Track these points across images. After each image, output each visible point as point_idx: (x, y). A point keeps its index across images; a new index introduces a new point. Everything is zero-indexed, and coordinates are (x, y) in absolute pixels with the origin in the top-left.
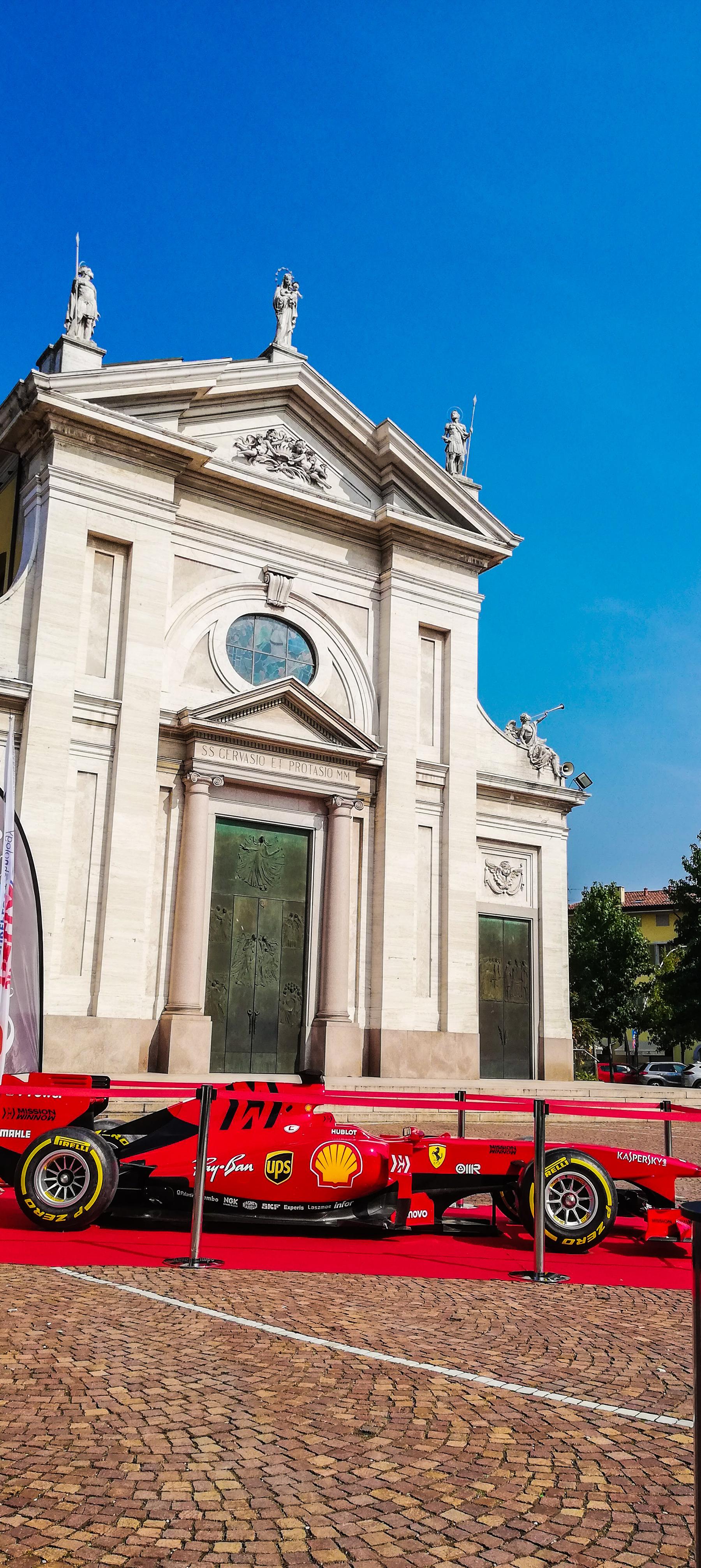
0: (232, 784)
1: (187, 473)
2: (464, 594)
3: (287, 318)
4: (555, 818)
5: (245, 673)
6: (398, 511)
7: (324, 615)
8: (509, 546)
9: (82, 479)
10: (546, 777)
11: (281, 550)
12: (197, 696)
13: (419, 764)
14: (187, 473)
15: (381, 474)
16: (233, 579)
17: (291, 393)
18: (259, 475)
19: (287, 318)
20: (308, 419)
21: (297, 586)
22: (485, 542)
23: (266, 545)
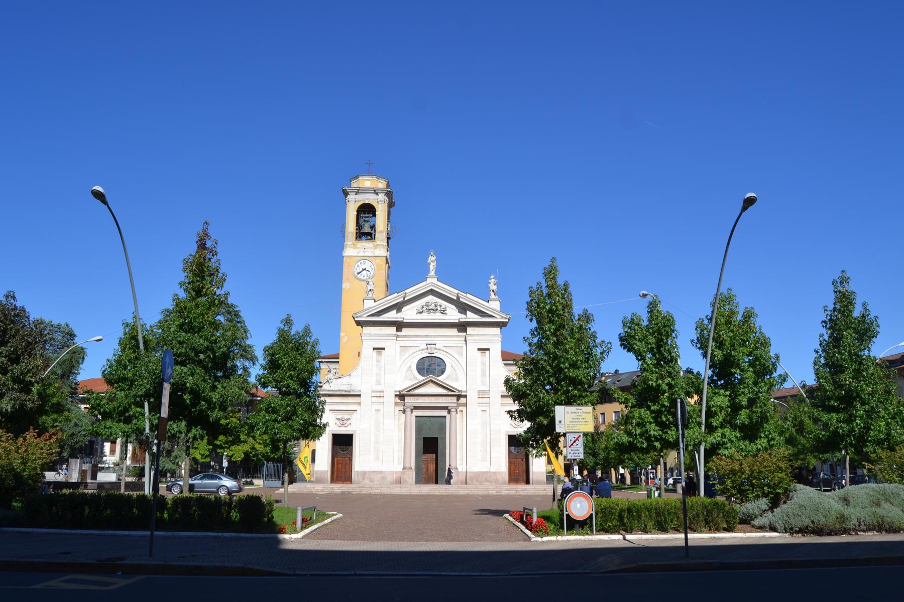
0: (416, 408)
1: (399, 326)
2: (494, 336)
3: (432, 266)
5: (423, 375)
6: (471, 317)
11: (431, 336)
12: (403, 385)
13: (479, 392)
14: (399, 326)
15: (463, 308)
19: (432, 266)
21: (437, 347)
22: (498, 319)
23: (427, 336)
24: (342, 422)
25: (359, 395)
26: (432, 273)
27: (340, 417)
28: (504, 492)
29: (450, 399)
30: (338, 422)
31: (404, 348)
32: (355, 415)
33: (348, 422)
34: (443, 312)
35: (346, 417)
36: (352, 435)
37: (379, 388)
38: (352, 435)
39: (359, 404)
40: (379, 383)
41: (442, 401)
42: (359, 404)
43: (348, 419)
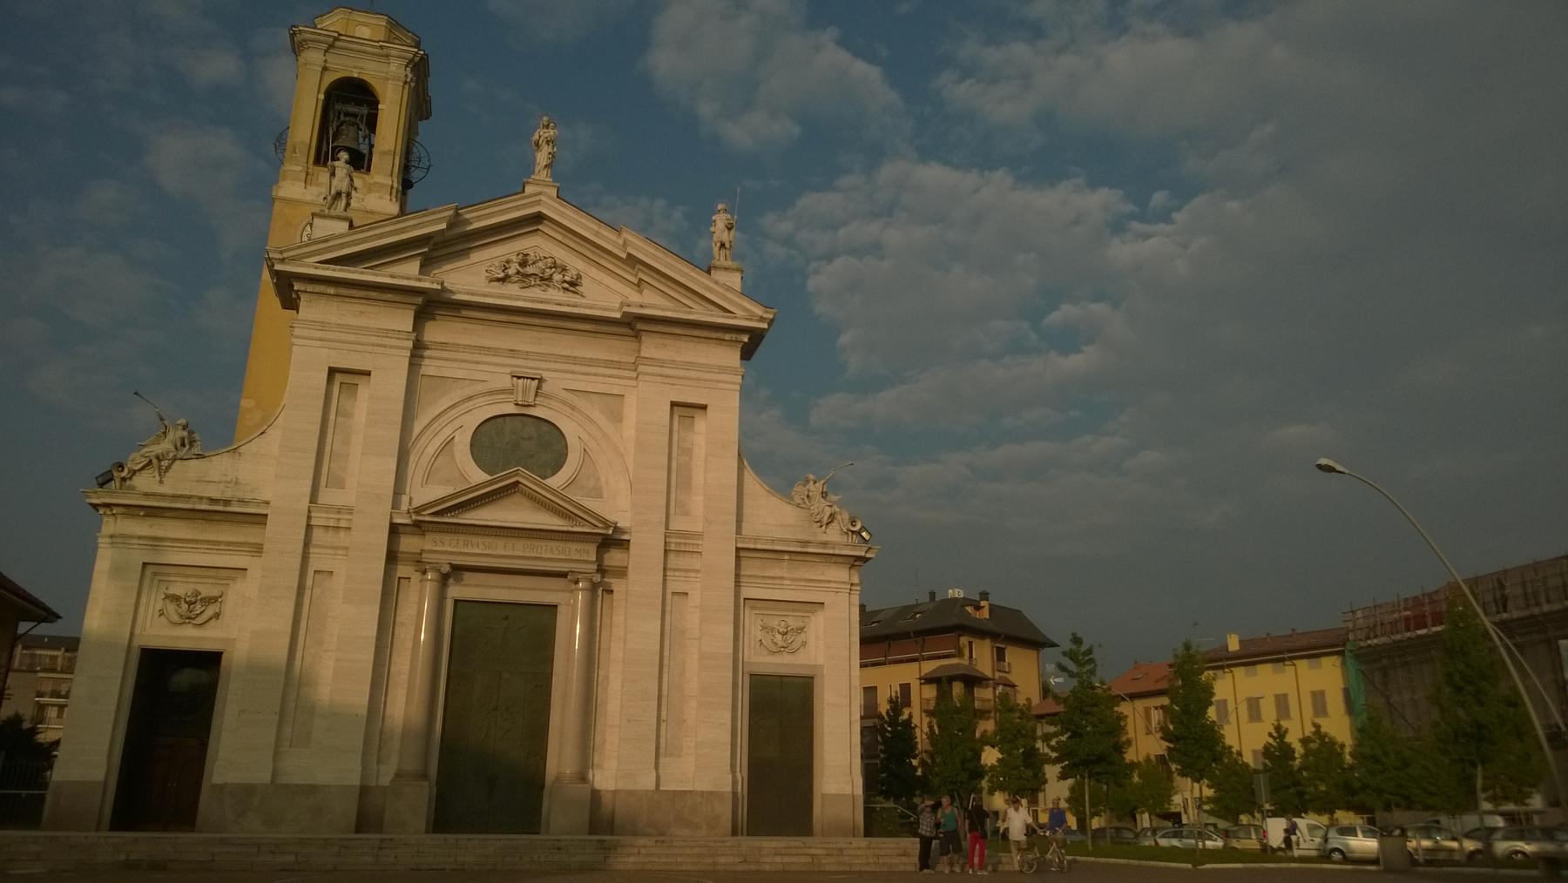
2: (722, 370)
4: (840, 574)
7: (573, 408)
8: (762, 319)
9: (323, 326)
10: (834, 535)
11: (527, 355)
16: (479, 388)
18: (512, 294)
20: (559, 237)
23: (513, 352)
25: (260, 519)
26: (542, 175)
28: (727, 861)
30: (171, 608)
33: (210, 611)
35: (206, 591)
36: (221, 654)
38: (221, 654)
42: (258, 549)
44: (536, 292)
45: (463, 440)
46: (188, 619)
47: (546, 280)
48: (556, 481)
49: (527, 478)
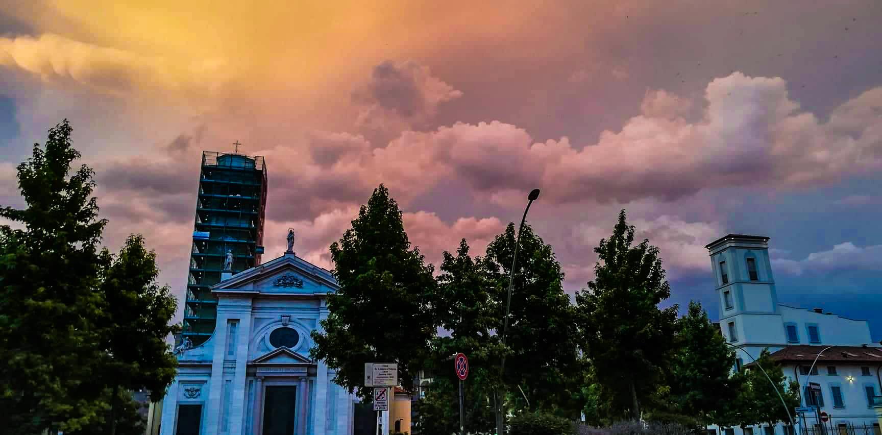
0: (267, 378)
9: (226, 306)
17: (289, 267)
23: (282, 308)
24: (192, 393)
27: (189, 387)
29: (301, 370)
30: (187, 394)
31: (257, 321)
32: (205, 386)
34: (300, 286)
35: (196, 387)
37: (231, 358)
39: (210, 375)
40: (231, 353)
41: (292, 372)
43: (198, 390)
44: (288, 289)
45: (268, 338)
46: (192, 396)
47: (291, 284)
48: (293, 349)
49: (284, 348)
